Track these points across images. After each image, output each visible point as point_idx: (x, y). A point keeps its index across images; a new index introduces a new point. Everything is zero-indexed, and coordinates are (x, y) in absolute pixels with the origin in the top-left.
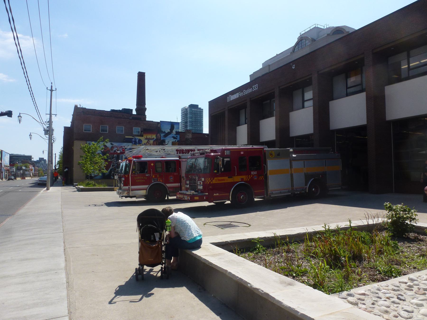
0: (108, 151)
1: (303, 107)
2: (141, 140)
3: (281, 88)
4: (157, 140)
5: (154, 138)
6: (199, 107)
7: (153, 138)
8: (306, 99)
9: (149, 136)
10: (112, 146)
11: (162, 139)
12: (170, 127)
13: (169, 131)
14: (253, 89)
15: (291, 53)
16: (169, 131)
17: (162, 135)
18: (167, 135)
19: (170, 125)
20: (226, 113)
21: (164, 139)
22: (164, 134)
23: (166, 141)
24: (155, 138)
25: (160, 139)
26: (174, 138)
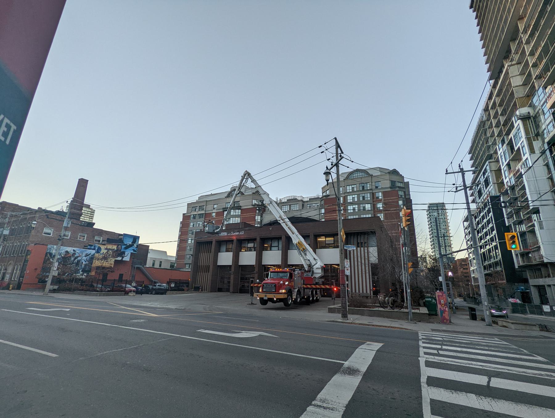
1: (271, 250)
2: (101, 249)
3: (261, 237)
4: (117, 250)
6: (91, 207)
7: (113, 248)
8: (272, 246)
9: (110, 247)
10: (74, 252)
11: (122, 250)
12: (132, 240)
13: (130, 243)
14: (239, 233)
16: (130, 243)
17: (123, 247)
18: (128, 247)
19: (133, 239)
20: (214, 243)
21: (124, 250)
23: (126, 253)
24: (116, 249)
25: (120, 250)
26: (134, 250)
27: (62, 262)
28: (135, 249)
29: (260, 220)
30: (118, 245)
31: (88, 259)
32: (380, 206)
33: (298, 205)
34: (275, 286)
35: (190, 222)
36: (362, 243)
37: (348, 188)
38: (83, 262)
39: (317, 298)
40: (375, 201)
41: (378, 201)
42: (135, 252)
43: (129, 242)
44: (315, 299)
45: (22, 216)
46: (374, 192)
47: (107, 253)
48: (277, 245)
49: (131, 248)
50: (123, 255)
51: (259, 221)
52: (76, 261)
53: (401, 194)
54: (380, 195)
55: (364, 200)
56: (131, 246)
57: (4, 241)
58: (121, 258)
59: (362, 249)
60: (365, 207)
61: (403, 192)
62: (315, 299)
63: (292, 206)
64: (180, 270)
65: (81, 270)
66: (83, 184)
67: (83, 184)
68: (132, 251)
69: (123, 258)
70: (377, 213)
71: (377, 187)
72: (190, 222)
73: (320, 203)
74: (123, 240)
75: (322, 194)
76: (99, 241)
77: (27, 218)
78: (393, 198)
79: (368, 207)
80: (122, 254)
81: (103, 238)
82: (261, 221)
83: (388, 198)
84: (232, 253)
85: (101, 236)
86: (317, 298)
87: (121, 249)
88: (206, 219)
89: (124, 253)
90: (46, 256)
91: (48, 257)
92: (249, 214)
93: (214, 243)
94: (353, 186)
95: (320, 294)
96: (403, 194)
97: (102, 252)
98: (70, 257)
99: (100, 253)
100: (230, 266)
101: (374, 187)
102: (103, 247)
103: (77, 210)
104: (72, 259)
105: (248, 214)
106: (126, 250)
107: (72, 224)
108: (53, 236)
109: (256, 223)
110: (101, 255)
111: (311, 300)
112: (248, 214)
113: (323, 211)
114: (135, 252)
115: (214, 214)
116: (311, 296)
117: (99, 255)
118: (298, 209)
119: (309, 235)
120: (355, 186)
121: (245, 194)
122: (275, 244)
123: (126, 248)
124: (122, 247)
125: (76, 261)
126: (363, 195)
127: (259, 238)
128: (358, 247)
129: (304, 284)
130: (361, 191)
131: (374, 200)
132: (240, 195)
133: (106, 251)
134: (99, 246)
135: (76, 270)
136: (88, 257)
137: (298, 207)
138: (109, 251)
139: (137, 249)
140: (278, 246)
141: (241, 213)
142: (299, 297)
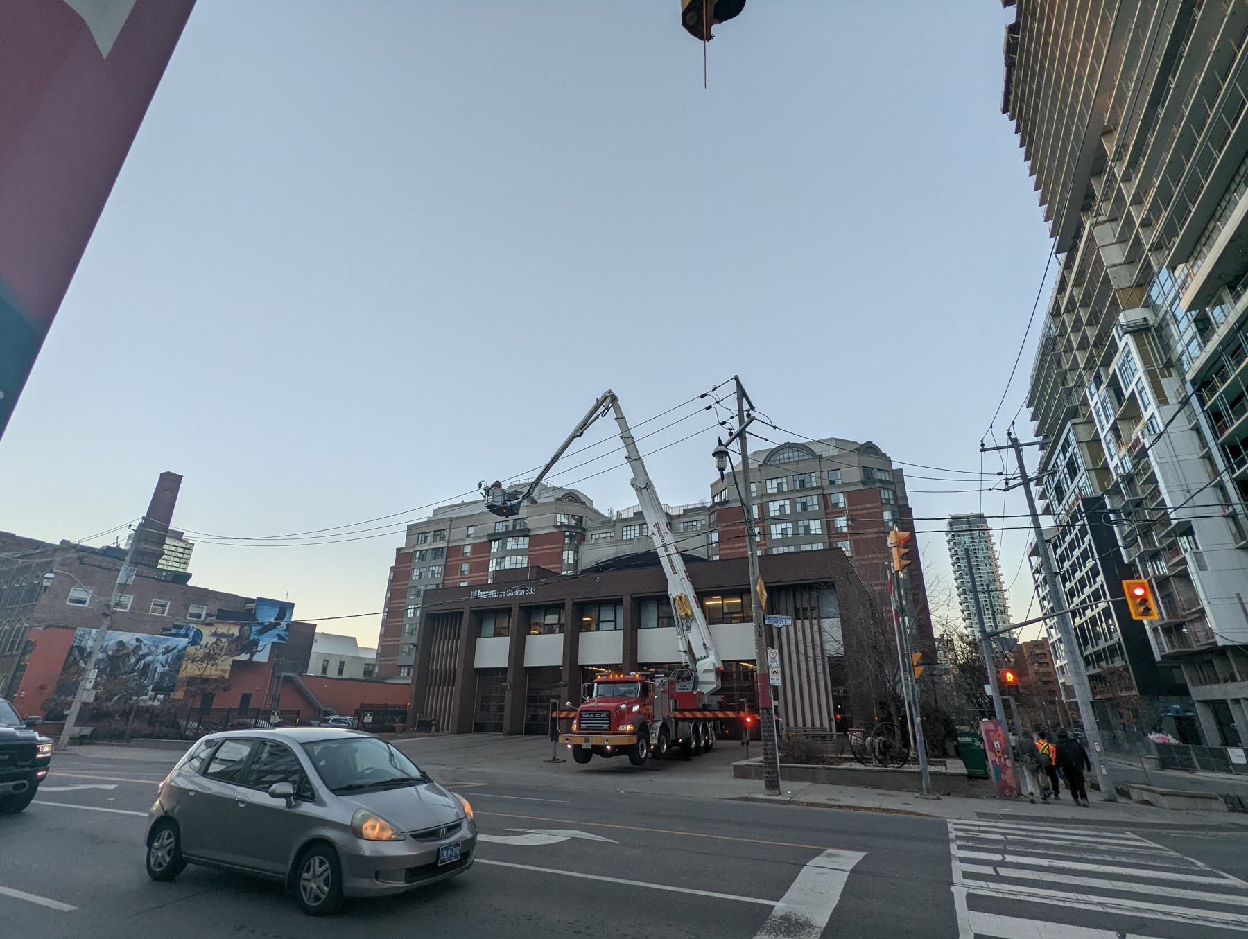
0: (124, 654)
1: (598, 629)
5: (233, 634)
7: (231, 633)
9: (223, 629)
11: (252, 638)
13: (272, 620)
14: (526, 591)
16: (272, 620)
17: (255, 629)
18: (265, 629)
20: (466, 616)
21: (257, 637)
22: (258, 628)
23: (261, 644)
24: (237, 634)
25: (248, 638)
26: (280, 637)
27: (105, 668)
28: (283, 634)
31: (169, 660)
32: (841, 523)
34: (609, 716)
36: (805, 609)
37: (769, 486)
38: (156, 668)
39: (707, 741)
41: (838, 512)
42: (281, 642)
43: (270, 616)
45: (21, 561)
46: (826, 492)
49: (275, 632)
51: (571, 561)
52: (141, 665)
53: (887, 497)
54: (841, 500)
55: (805, 513)
56: (273, 626)
58: (248, 655)
59: (807, 622)
60: (809, 526)
61: (890, 492)
64: (387, 681)
66: (169, 485)
67: (169, 485)
68: (276, 640)
69: (252, 655)
74: (255, 614)
75: (711, 500)
76: (199, 616)
77: (33, 566)
78: (870, 505)
79: (816, 526)
80: (251, 647)
82: (576, 562)
83: (859, 507)
84: (507, 640)
85: (205, 605)
86: (707, 741)
87: (250, 635)
89: (256, 643)
90: (70, 655)
91: (75, 659)
93: (466, 616)
94: (780, 481)
96: (891, 497)
97: (203, 642)
98: (128, 655)
99: (198, 644)
100: (503, 670)
101: (826, 483)
102: (206, 631)
104: (133, 660)
105: (545, 547)
106: (261, 637)
107: (140, 578)
108: (90, 608)
109: (564, 567)
110: (202, 650)
111: (693, 747)
112: (545, 547)
113: (715, 537)
114: (281, 642)
115: (468, 549)
116: (693, 737)
120: (784, 480)
121: (539, 501)
122: (607, 614)
123: (261, 632)
124: (251, 630)
125: (141, 665)
126: (804, 500)
127: (571, 603)
128: (798, 618)
129: (675, 709)
130: (797, 491)
131: (828, 511)
133: (214, 639)
135: (139, 687)
136: (170, 654)
140: (615, 621)
141: (530, 545)
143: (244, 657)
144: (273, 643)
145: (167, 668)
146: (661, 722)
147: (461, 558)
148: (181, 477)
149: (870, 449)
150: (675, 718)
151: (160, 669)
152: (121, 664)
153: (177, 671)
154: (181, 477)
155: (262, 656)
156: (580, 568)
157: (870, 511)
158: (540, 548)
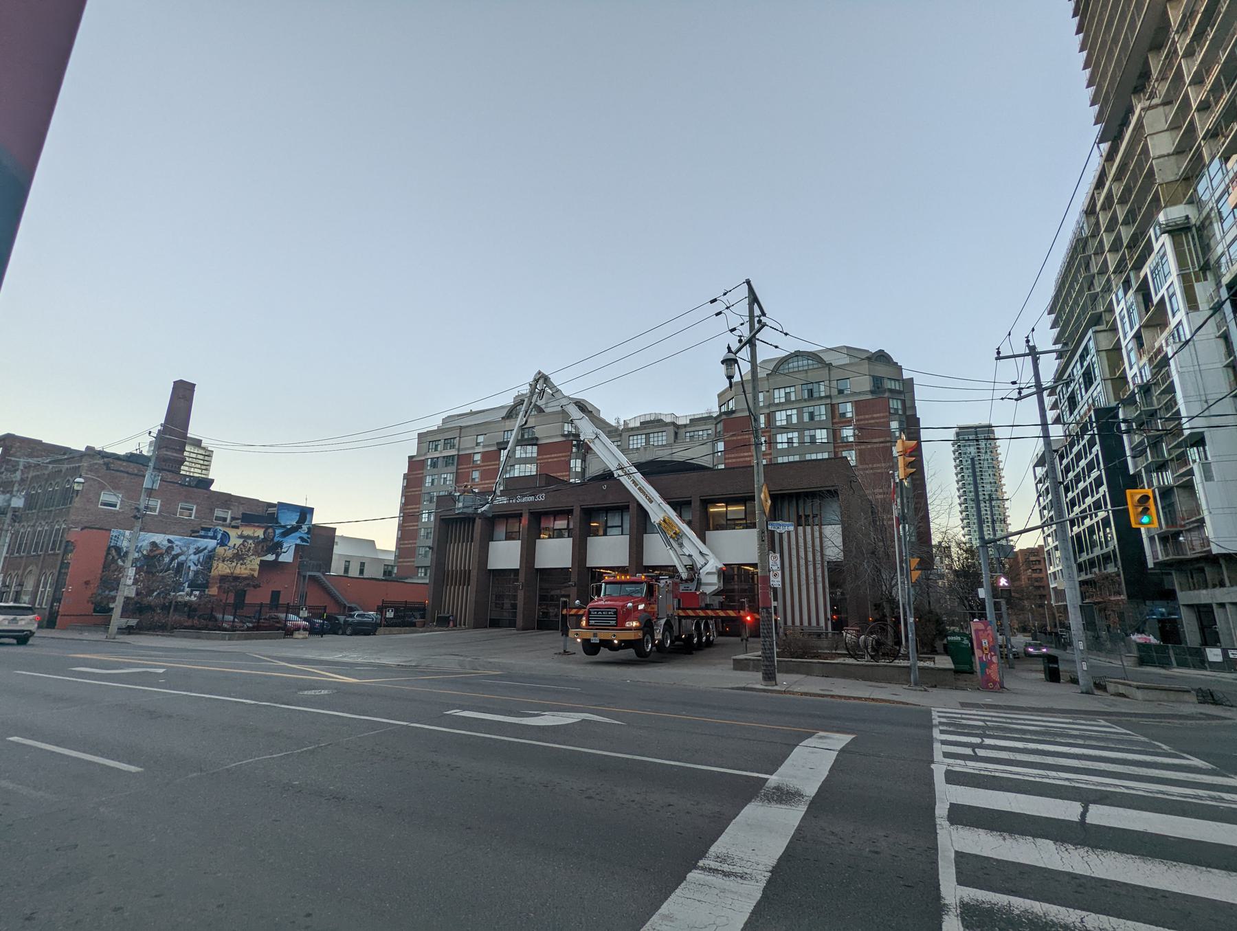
1: (605, 534)
2: (229, 538)
3: (582, 507)
4: (265, 540)
6: (203, 445)
7: (256, 535)
8: (609, 524)
9: (248, 531)
11: (276, 539)
15: (503, 418)
17: (278, 532)
18: (288, 532)
23: (285, 545)
25: (273, 540)
26: (302, 539)
27: (143, 566)
28: (305, 536)
29: (581, 468)
30: (267, 528)
31: (201, 560)
32: (848, 433)
33: (664, 434)
34: (615, 613)
35: (425, 474)
36: (807, 516)
37: (776, 395)
38: (190, 567)
39: (708, 638)
40: (836, 423)
41: (846, 422)
42: (304, 544)
44: (704, 641)
45: (51, 466)
46: (834, 402)
47: (244, 546)
48: (620, 524)
49: (297, 534)
50: (280, 551)
51: (579, 469)
52: (175, 564)
53: (895, 407)
54: (849, 409)
56: (295, 529)
57: (15, 521)
58: (274, 556)
59: (808, 529)
60: (815, 436)
61: (899, 402)
62: (704, 641)
63: (651, 435)
64: (406, 581)
65: (187, 583)
66: (183, 393)
67: (183, 393)
68: (298, 542)
69: (278, 555)
70: (841, 449)
71: (841, 392)
72: (425, 474)
73: (714, 429)
74: (277, 518)
75: (718, 409)
76: (225, 519)
77: (64, 471)
78: (878, 415)
79: (822, 435)
80: (276, 548)
81: (232, 512)
82: (584, 470)
83: (867, 417)
85: (229, 509)
86: (708, 638)
88: (460, 467)
89: (280, 545)
90: (108, 554)
91: (113, 557)
92: (556, 455)
94: (788, 390)
95: (714, 630)
96: (900, 407)
97: (231, 544)
98: (162, 555)
100: (516, 571)
101: (834, 392)
102: (233, 533)
103: (173, 452)
104: (167, 560)
105: (553, 456)
108: (121, 511)
110: (231, 551)
111: (695, 642)
112: (553, 456)
113: (721, 446)
114: (304, 544)
115: (478, 457)
116: (695, 634)
117: (225, 550)
118: (664, 443)
119: (691, 501)
120: (793, 389)
121: (547, 410)
122: (614, 520)
124: (274, 532)
125: (175, 564)
126: (811, 409)
127: (579, 509)
129: (679, 608)
130: (805, 400)
131: (835, 421)
132: (536, 413)
133: (241, 541)
134: (224, 531)
136: (202, 554)
137: (664, 438)
138: (248, 541)
139: (309, 536)
140: (622, 526)
141: (538, 454)
142: (669, 637)
143: (270, 557)
144: (296, 545)
145: (199, 566)
146: (665, 620)
147: (471, 466)
148: (194, 385)
149: (882, 357)
150: (679, 616)
151: (193, 568)
152: (156, 563)
153: (210, 570)
154: (194, 385)
155: (287, 557)
156: (587, 476)
157: (877, 421)
158: (548, 456)
